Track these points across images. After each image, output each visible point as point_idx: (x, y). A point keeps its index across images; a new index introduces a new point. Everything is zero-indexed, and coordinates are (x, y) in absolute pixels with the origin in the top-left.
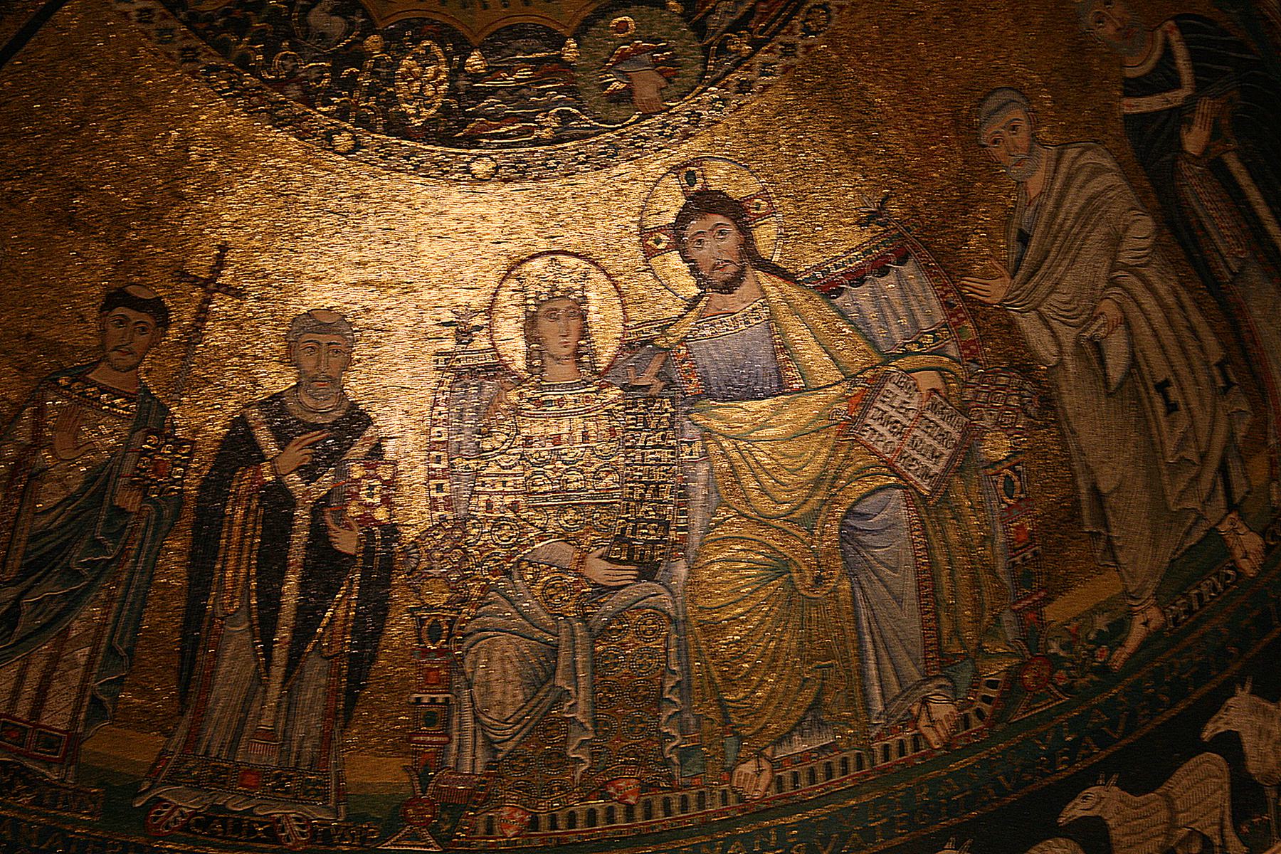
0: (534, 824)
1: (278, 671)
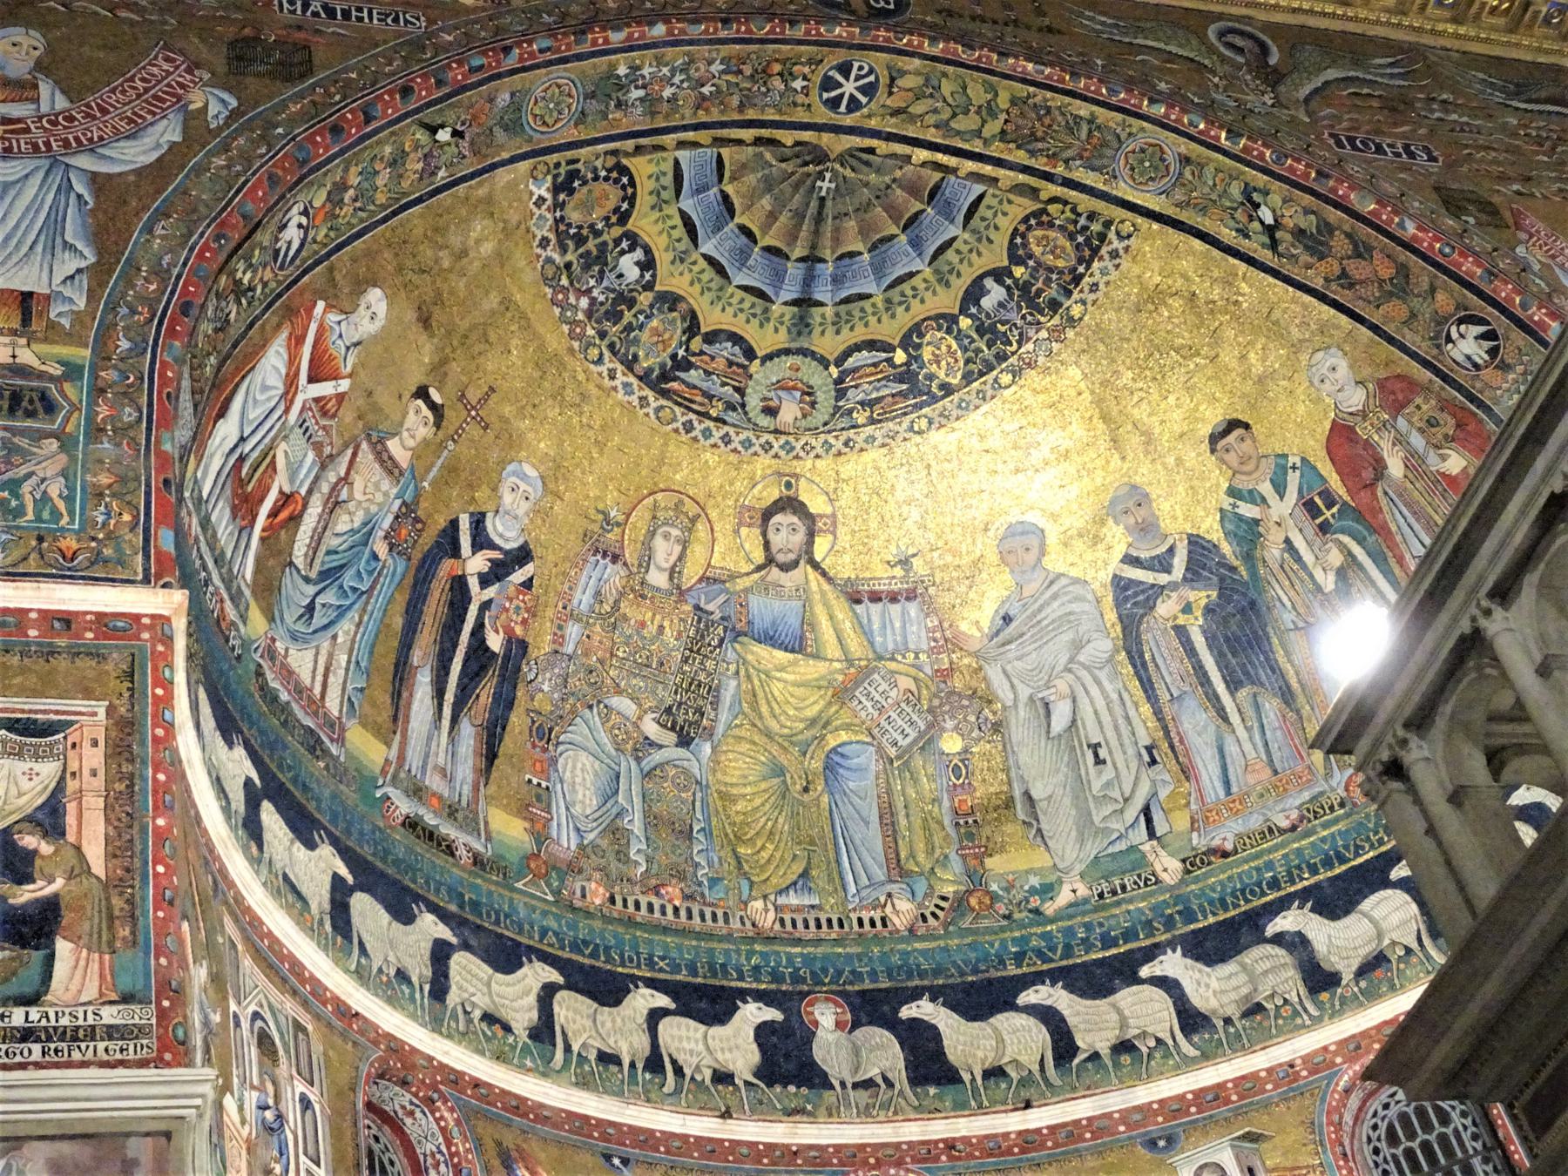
0: (612, 900)
1: (446, 723)
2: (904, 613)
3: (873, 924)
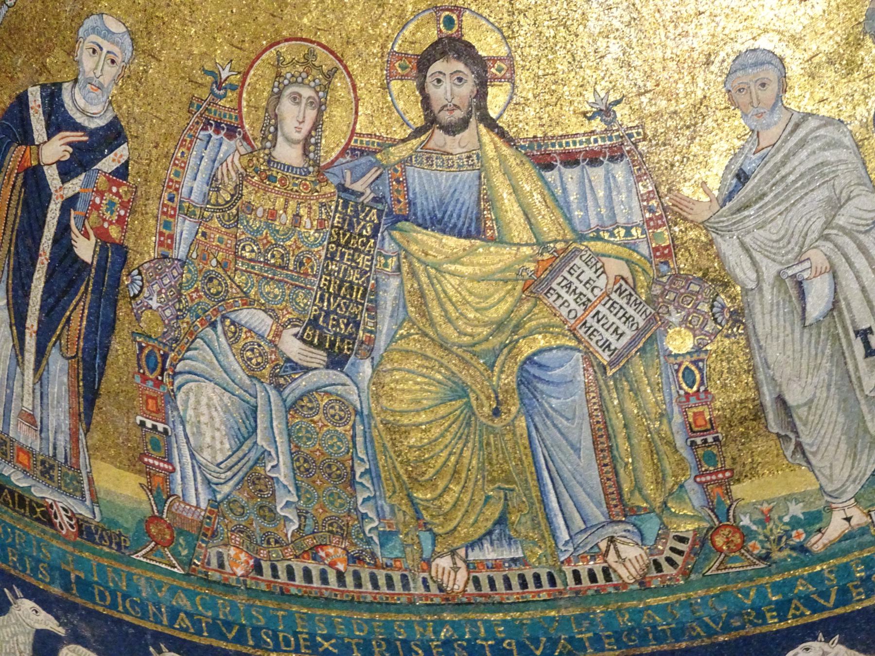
1: (30, 356)
2: (609, 178)
3: (593, 577)
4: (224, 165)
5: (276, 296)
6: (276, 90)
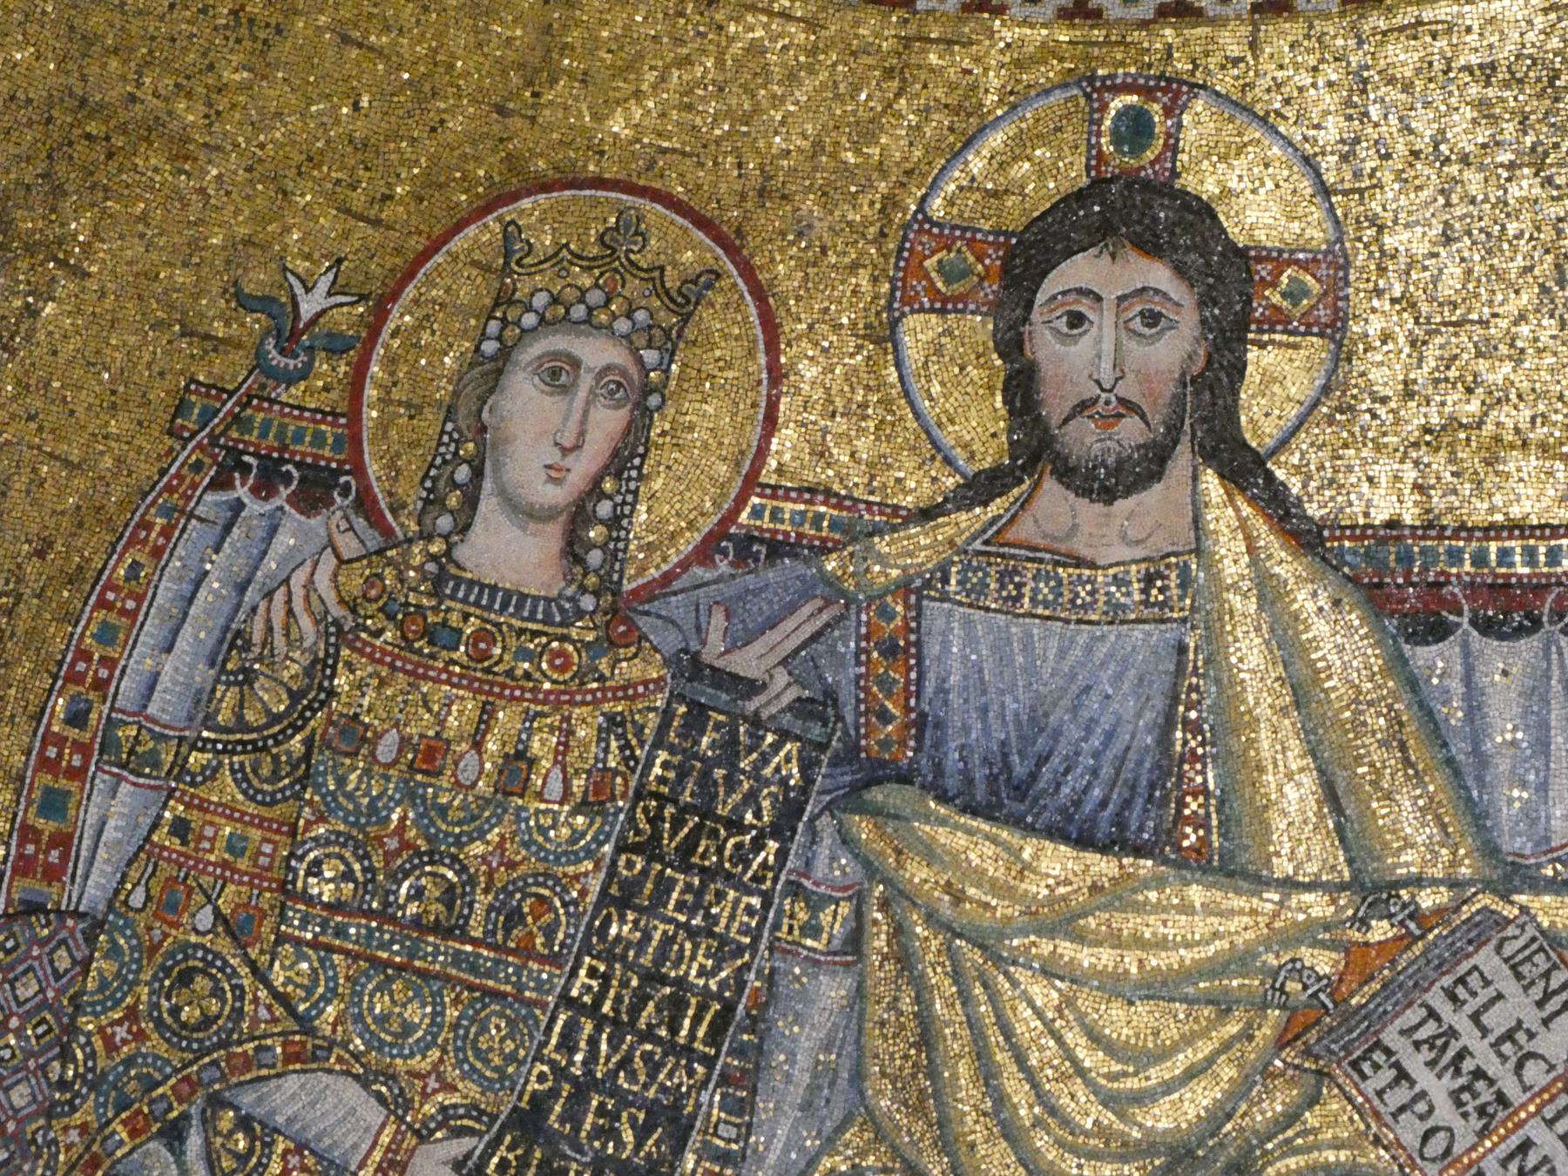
4: (280, 596)
5: (408, 1029)
6: (489, 347)
